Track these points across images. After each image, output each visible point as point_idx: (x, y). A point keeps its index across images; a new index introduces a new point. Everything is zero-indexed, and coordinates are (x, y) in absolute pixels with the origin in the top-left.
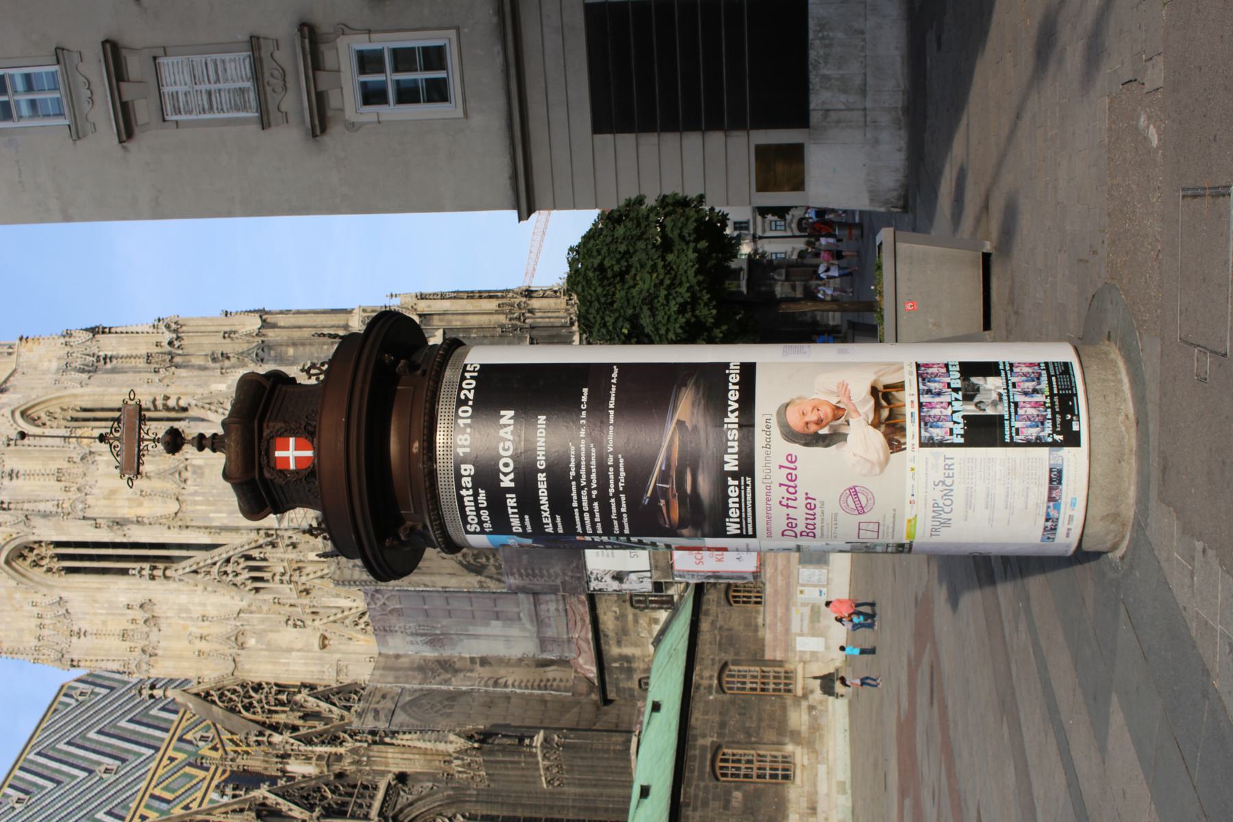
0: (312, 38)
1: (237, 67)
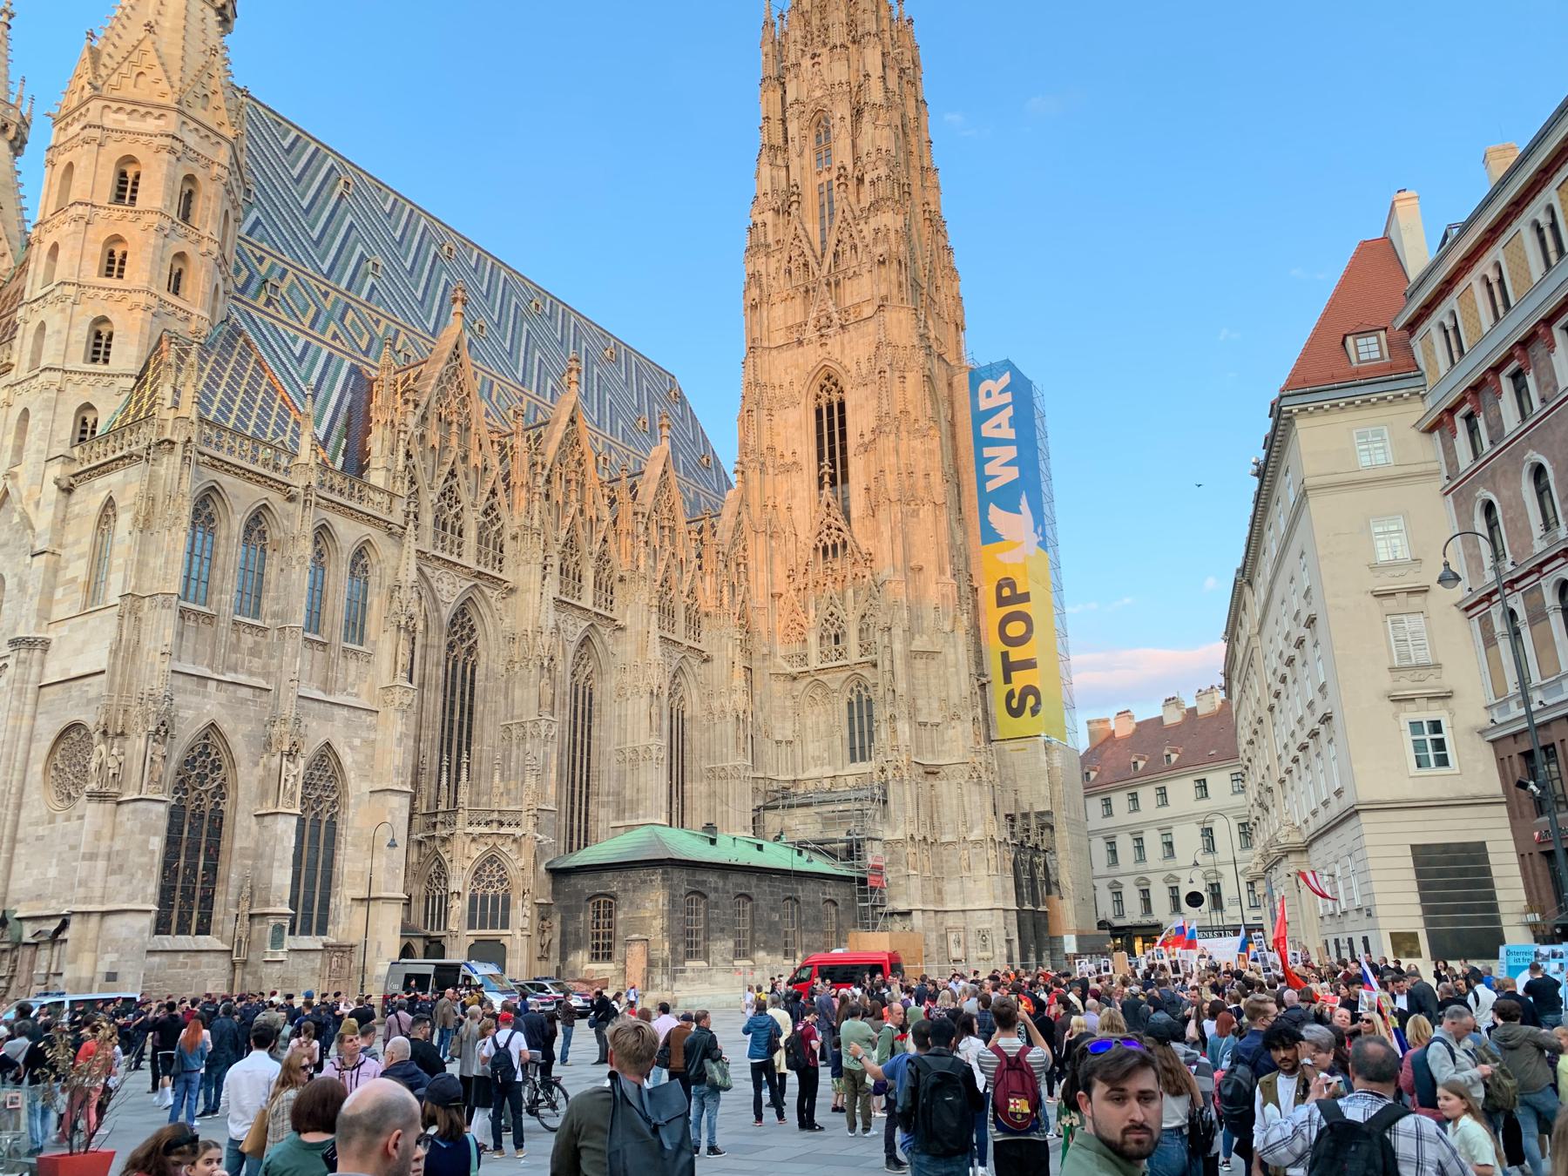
1: (1424, 656)
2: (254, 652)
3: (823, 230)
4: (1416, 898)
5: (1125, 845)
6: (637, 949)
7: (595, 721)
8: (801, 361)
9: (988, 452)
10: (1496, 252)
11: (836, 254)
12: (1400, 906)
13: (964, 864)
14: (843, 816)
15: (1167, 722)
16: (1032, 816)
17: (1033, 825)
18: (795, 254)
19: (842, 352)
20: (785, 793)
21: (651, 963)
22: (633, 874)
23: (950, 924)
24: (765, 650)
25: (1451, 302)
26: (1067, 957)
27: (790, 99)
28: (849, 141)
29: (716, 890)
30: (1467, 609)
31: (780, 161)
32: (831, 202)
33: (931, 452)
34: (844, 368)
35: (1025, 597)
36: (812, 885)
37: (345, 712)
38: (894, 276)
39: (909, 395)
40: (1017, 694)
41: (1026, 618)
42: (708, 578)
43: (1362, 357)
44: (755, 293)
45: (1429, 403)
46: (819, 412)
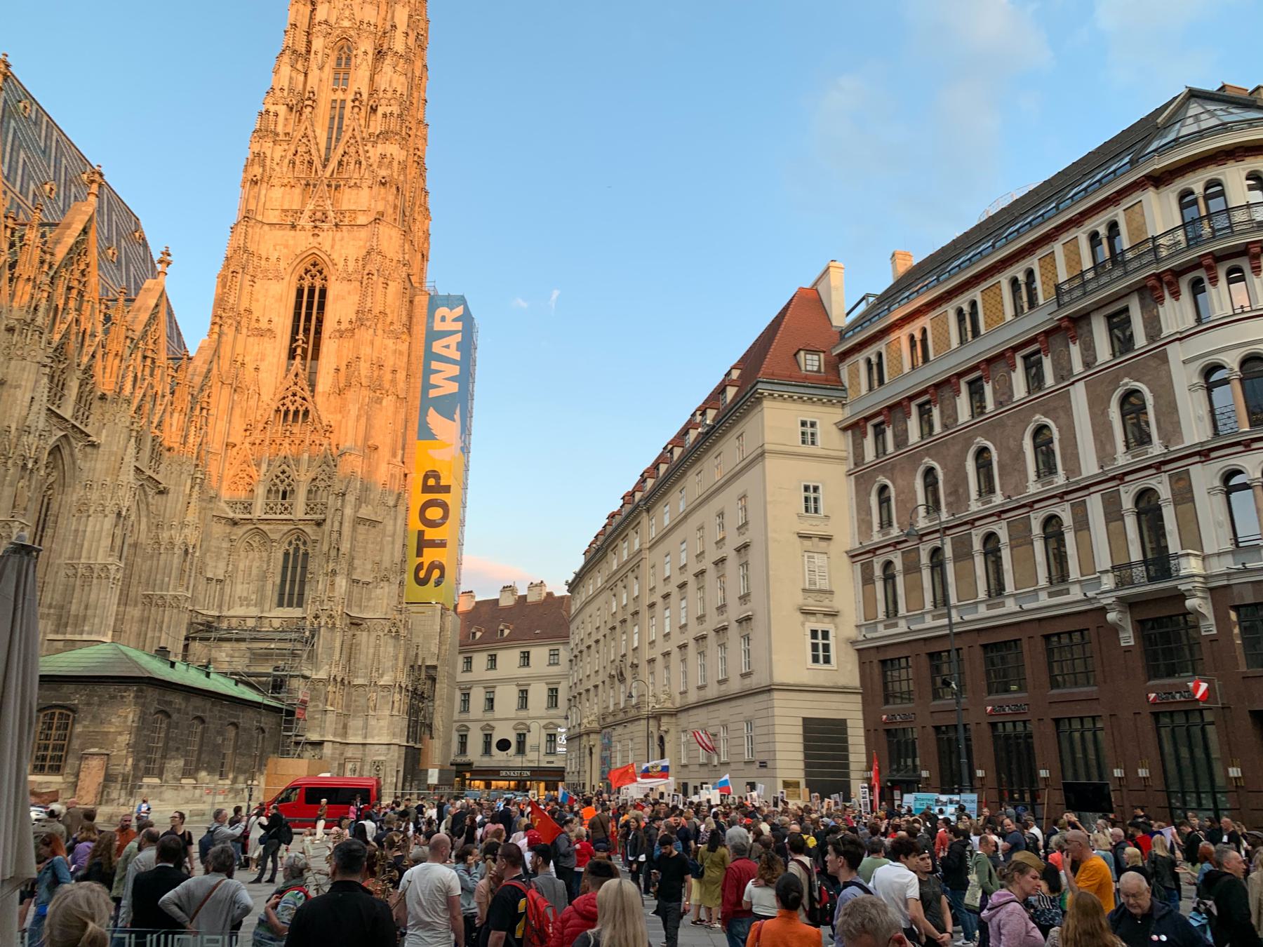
0: (833, 615)
1: (822, 584)
3: (330, 138)
4: (801, 756)
5: (478, 697)
6: (95, 763)
7: (49, 532)
8: (291, 242)
9: (435, 365)
10: (925, 321)
11: (340, 164)
12: (790, 760)
13: (372, 704)
14: (266, 656)
15: (502, 603)
16: (423, 668)
17: (423, 676)
18: (302, 149)
19: (332, 247)
20: (209, 626)
21: (109, 778)
22: (100, 689)
23: (349, 754)
24: (212, 493)
25: (881, 346)
26: (429, 787)
27: (321, 14)
28: (368, 74)
29: (179, 711)
30: (853, 556)
31: (299, 66)
32: (341, 118)
33: (401, 353)
34: (332, 261)
35: (447, 489)
36: (250, 713)
38: (391, 198)
39: (390, 299)
40: (425, 567)
41: (444, 506)
42: (176, 415)
43: (809, 368)
44: (257, 170)
45: (847, 412)
46: (300, 292)
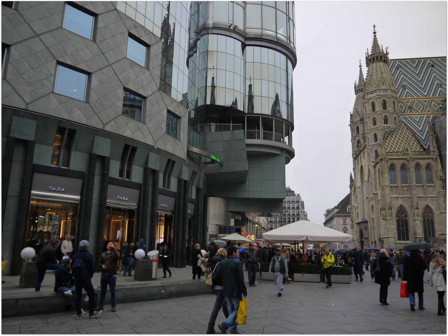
2: (407, 190)
37: (430, 198)
